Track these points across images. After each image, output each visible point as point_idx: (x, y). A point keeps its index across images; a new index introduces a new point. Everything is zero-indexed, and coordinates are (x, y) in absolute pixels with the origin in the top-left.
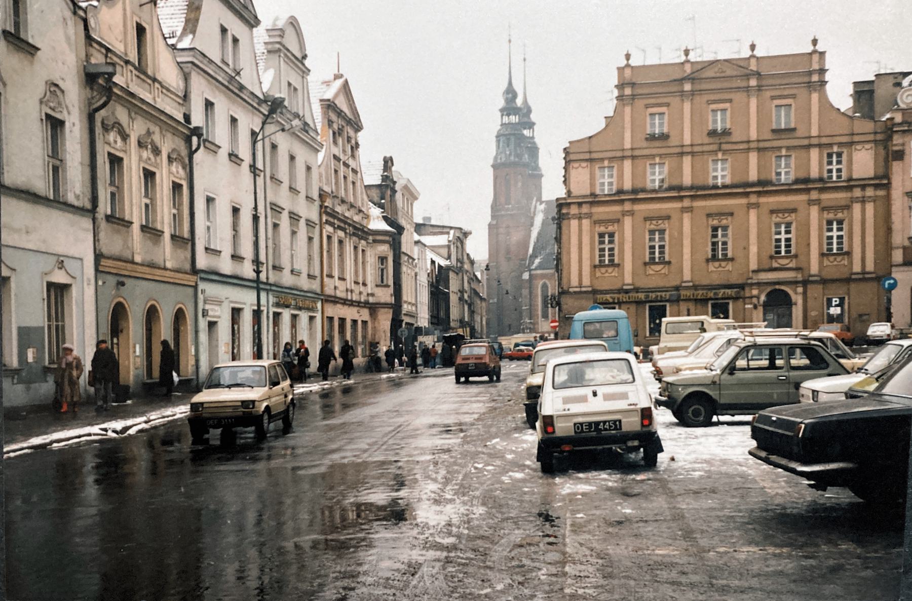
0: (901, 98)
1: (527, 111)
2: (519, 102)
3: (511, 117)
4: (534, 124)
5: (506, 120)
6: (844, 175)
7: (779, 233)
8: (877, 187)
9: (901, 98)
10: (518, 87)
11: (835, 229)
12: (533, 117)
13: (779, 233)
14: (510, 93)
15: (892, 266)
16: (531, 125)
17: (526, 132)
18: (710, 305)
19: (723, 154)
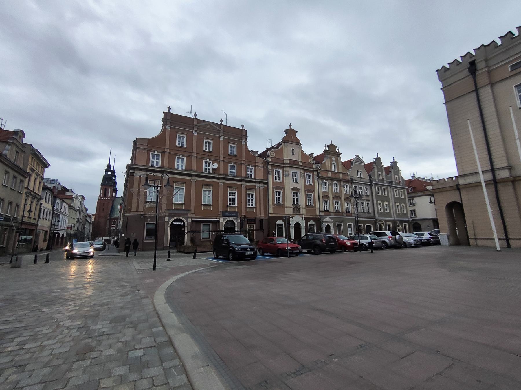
0: (270, 154)
1: (113, 172)
2: (112, 169)
4: (116, 176)
5: (107, 173)
6: (253, 177)
7: (231, 196)
8: (264, 183)
9: (270, 154)
11: (250, 197)
12: (116, 174)
13: (231, 196)
14: (109, 166)
15: (242, 215)
16: (115, 176)
17: (114, 178)
18: (202, 225)
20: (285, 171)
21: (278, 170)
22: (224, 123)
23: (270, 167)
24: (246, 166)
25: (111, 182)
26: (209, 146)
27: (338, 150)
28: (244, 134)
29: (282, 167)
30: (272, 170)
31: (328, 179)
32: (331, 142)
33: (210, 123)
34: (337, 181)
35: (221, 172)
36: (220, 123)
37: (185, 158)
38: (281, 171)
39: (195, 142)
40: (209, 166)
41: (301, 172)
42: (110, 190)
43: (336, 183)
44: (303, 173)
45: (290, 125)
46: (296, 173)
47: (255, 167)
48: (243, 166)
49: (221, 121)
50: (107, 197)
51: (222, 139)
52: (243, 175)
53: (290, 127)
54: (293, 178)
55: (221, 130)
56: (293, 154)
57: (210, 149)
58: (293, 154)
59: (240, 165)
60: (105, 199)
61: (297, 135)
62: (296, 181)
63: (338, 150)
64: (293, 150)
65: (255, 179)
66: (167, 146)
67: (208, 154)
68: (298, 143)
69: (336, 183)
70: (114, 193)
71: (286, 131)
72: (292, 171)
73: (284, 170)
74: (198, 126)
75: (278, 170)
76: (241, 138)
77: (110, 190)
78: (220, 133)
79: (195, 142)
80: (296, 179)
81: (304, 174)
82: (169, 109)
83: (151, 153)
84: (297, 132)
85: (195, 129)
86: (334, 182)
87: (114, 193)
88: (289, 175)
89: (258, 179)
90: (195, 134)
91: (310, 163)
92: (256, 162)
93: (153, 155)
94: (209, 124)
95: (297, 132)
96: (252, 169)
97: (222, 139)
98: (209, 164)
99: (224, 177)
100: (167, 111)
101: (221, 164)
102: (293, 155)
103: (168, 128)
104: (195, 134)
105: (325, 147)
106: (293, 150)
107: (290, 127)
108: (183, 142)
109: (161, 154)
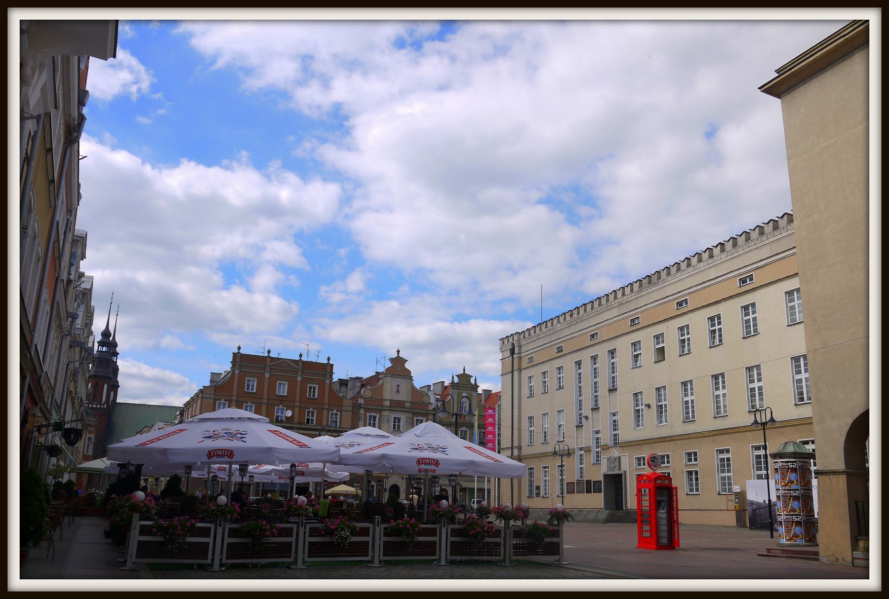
3: (105, 348)
4: (118, 354)
10: (111, 330)
19: (282, 406)
20: (384, 416)
21: (373, 414)
22: (304, 359)
23: (362, 411)
24: (328, 411)
25: (109, 370)
26: (283, 390)
27: (476, 380)
28: (328, 370)
29: (379, 411)
30: (365, 415)
31: (451, 425)
32: (464, 370)
33: (287, 361)
34: (466, 427)
35: (296, 420)
36: (298, 358)
37: (254, 405)
38: (378, 415)
39: (266, 385)
40: (282, 413)
41: (407, 417)
42: (106, 386)
43: (466, 429)
44: (410, 418)
45: (398, 352)
46: (399, 419)
47: (341, 412)
48: (325, 412)
49: (301, 356)
50: (100, 403)
51: (299, 379)
52: (324, 423)
53: (398, 354)
54: (394, 425)
55: (299, 368)
56: (398, 391)
57: (284, 392)
58: (398, 391)
59: (320, 411)
60: (96, 408)
61: (407, 366)
62: (399, 428)
63: (476, 380)
64: (398, 386)
65: (340, 427)
66: (235, 393)
67: (281, 400)
68: (407, 375)
69: (466, 429)
70: (112, 394)
71: (392, 360)
72: (393, 416)
73: (382, 414)
74: (271, 366)
75: (373, 414)
76: (325, 376)
77: (106, 386)
78: (297, 371)
79: (266, 385)
80: (399, 426)
81: (413, 418)
82: (239, 348)
83: (217, 402)
84: (407, 360)
85: (268, 369)
86: (462, 429)
87: (112, 394)
88: (388, 421)
89: (344, 428)
90: (267, 375)
91: (424, 403)
92: (342, 406)
93: (220, 404)
94: (285, 361)
95: (407, 360)
96: (336, 414)
97: (299, 379)
98: (282, 410)
99: (299, 426)
100: (236, 351)
101: (297, 410)
102: (398, 394)
103: (237, 372)
104: (267, 375)
105: (453, 377)
106: (398, 386)
107: (398, 354)
108: (253, 386)
109: (227, 403)
